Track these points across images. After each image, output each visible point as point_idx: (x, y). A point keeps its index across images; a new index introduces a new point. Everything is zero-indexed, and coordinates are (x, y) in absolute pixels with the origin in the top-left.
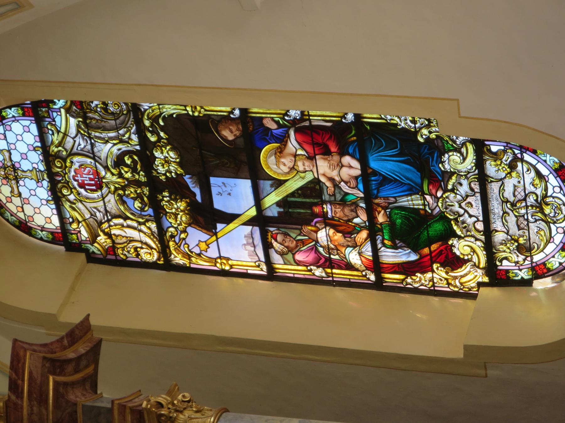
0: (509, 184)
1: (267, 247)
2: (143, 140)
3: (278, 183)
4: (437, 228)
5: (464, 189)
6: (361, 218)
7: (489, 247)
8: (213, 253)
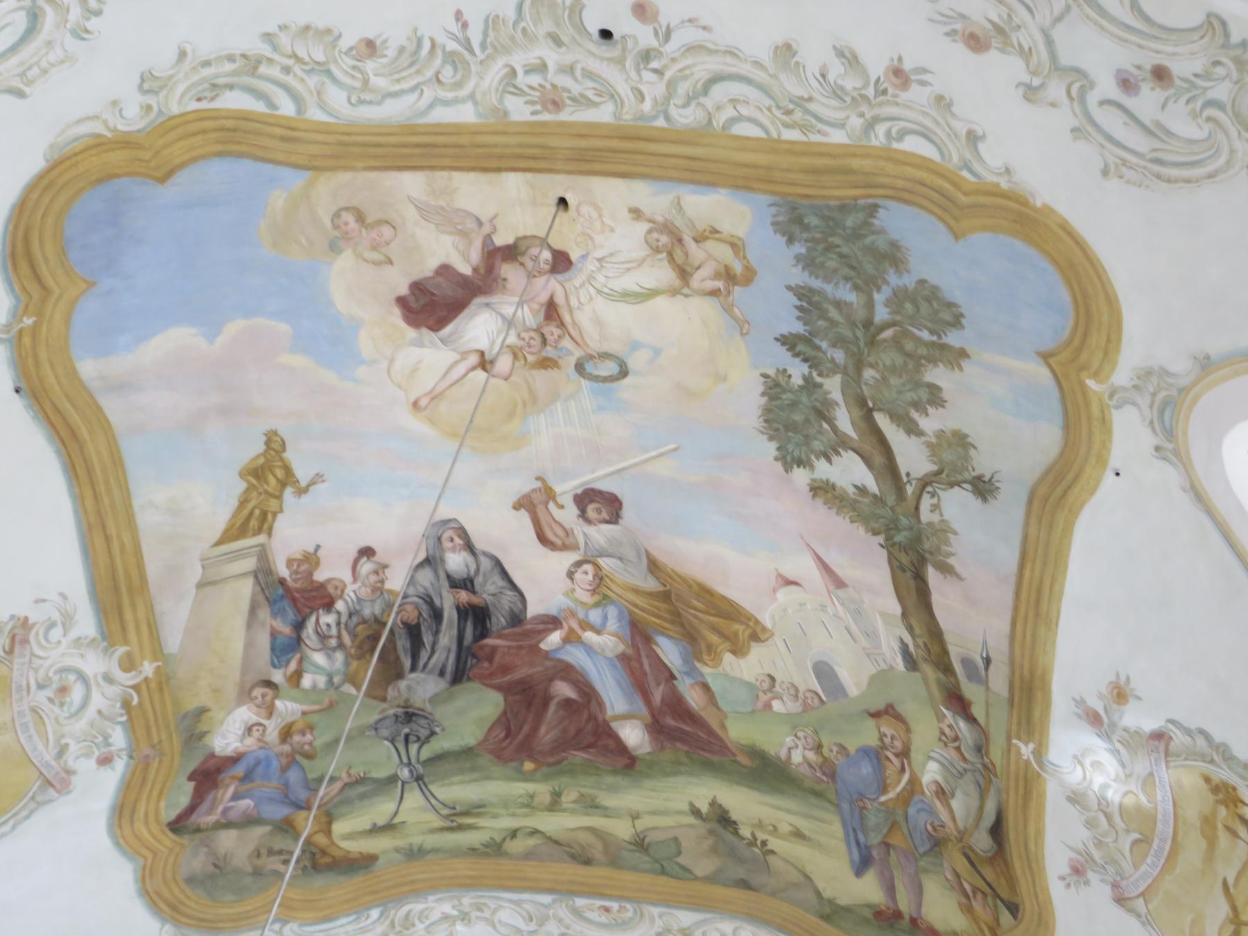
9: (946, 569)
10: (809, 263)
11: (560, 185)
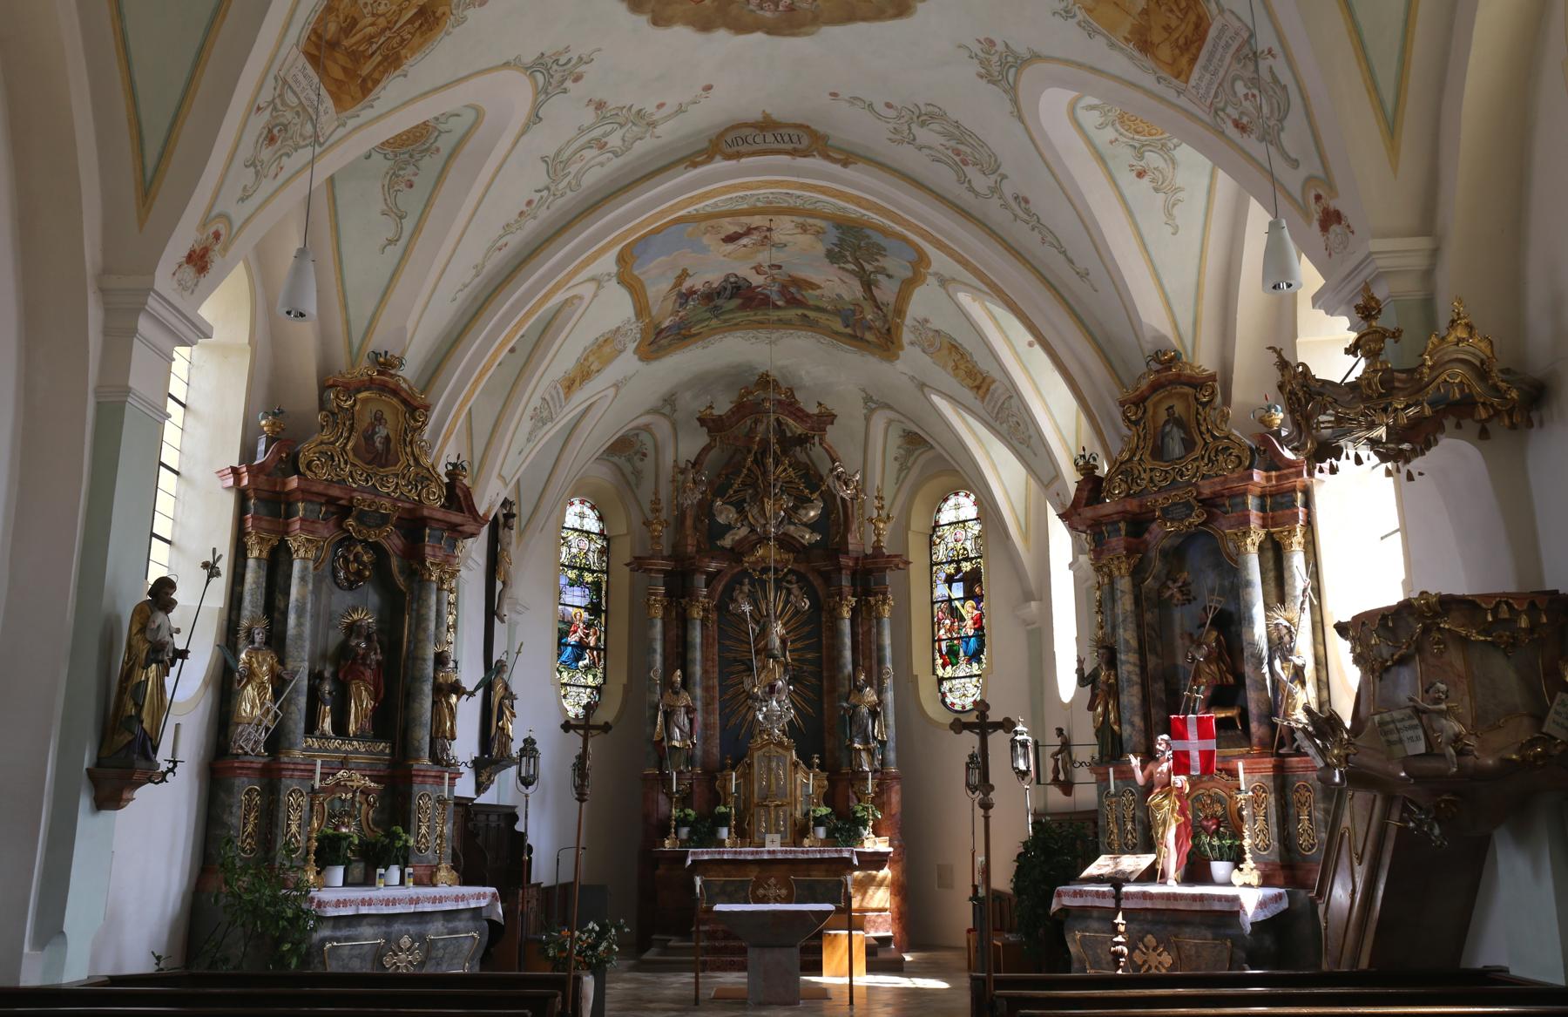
0: (970, 685)
1: (942, 602)
2: (973, 559)
3: (963, 607)
5: (967, 670)
6: (955, 636)
8: (938, 582)
9: (877, 287)
10: (843, 233)
11: (770, 217)
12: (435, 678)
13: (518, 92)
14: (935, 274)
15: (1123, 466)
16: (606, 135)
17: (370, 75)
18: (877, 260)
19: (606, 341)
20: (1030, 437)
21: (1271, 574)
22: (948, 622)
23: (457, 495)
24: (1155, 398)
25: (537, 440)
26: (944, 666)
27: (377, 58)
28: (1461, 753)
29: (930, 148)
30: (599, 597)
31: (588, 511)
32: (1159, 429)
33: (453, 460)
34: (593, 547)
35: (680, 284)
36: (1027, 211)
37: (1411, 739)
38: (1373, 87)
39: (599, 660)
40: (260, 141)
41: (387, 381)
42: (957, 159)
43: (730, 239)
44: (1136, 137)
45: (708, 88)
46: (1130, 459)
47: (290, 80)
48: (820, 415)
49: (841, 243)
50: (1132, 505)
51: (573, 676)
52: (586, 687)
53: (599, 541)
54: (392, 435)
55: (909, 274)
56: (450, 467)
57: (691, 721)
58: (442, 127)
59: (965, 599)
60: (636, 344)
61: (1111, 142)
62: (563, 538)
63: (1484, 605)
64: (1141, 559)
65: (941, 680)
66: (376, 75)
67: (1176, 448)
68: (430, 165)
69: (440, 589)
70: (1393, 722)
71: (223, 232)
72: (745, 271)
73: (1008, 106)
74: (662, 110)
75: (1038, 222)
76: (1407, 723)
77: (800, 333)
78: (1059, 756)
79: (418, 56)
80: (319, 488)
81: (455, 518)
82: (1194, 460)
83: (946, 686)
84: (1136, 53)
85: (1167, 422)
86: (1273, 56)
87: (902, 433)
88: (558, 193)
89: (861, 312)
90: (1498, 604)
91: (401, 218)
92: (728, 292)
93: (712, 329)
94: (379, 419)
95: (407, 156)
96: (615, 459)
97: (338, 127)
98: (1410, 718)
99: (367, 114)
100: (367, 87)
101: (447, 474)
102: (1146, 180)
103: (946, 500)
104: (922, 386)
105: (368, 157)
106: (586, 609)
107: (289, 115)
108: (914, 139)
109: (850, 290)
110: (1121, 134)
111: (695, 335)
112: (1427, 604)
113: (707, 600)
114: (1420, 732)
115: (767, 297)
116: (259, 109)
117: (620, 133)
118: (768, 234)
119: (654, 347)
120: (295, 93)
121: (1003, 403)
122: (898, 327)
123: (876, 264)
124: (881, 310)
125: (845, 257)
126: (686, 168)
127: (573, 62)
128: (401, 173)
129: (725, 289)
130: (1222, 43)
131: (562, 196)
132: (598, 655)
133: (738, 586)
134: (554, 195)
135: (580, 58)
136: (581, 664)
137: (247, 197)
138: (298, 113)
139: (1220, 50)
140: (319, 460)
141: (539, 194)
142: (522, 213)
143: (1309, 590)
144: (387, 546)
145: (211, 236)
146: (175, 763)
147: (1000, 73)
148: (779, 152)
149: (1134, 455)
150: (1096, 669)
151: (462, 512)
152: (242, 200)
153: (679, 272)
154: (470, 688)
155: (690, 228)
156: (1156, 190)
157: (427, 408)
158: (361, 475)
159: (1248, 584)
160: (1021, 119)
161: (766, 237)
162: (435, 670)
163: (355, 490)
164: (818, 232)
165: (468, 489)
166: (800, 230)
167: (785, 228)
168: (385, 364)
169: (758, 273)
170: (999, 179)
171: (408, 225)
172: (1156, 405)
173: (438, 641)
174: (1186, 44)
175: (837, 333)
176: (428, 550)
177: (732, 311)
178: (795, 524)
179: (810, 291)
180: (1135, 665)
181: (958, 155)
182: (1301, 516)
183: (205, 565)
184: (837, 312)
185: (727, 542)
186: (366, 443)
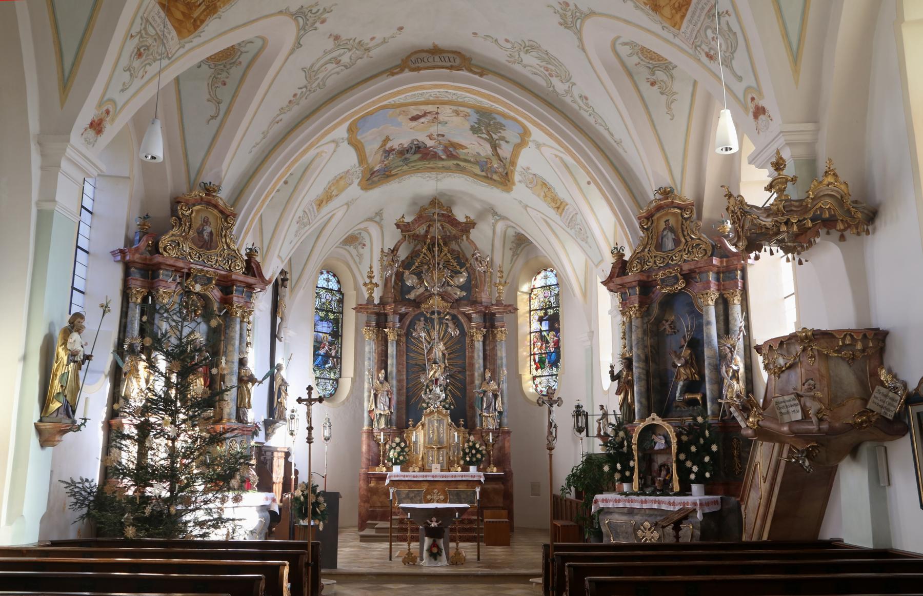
1: (536, 332)
2: (554, 307)
3: (548, 335)
4: (543, 366)
6: (543, 352)
7: (540, 376)
9: (500, 148)
11: (438, 106)
12: (239, 373)
13: (288, 31)
14: (534, 141)
15: (639, 254)
16: (340, 55)
17: (198, 17)
18: (500, 132)
19: (341, 178)
20: (587, 237)
21: (722, 318)
22: (539, 344)
23: (253, 268)
24: (658, 215)
25: (300, 236)
26: (537, 369)
27: (203, 7)
28: (821, 420)
29: (531, 66)
30: (338, 328)
31: (331, 278)
32: (660, 233)
33: (250, 246)
34: (334, 298)
35: (385, 145)
36: (587, 105)
37: (794, 411)
38: (786, 35)
39: (338, 364)
40: (133, 55)
41: (211, 199)
42: (547, 73)
43: (414, 118)
44: (651, 62)
45: (401, 29)
46: (643, 250)
47: (150, 19)
48: (466, 223)
49: (479, 122)
50: (644, 278)
51: (322, 373)
52: (330, 379)
53: (338, 295)
54: (214, 231)
55: (518, 141)
56: (248, 251)
57: (390, 399)
58: (243, 49)
59: (549, 331)
60: (359, 180)
61: (636, 65)
62: (317, 293)
63: (837, 336)
64: (648, 308)
65: (534, 378)
66: (202, 17)
67: (669, 244)
68: (236, 72)
69: (242, 322)
70: (784, 402)
71: (111, 110)
72: (422, 138)
73: (577, 42)
74: (373, 41)
75: (593, 111)
76: (792, 403)
77: (455, 175)
78: (601, 421)
79: (227, 6)
80: (171, 262)
81: (251, 280)
82: (680, 251)
83: (538, 380)
84: (650, 12)
85: (665, 229)
86: (729, 15)
87: (514, 234)
88: (312, 90)
89: (491, 163)
90: (845, 335)
91: (219, 103)
92: (413, 150)
93: (404, 172)
94: (206, 222)
95: (222, 66)
96: (347, 247)
97: (179, 48)
98: (794, 399)
99: (197, 41)
100: (197, 24)
101: (247, 254)
102: (656, 87)
103: (539, 273)
104: (526, 207)
105: (199, 66)
106: (330, 334)
107: (150, 41)
108: (522, 61)
109: (486, 150)
110: (642, 60)
111: (394, 175)
112: (806, 335)
113: (399, 330)
114: (799, 408)
115: (436, 153)
116: (132, 36)
117: (349, 54)
118: (436, 116)
119: (370, 182)
120: (153, 27)
121: (572, 217)
122: (512, 171)
123: (499, 134)
124: (502, 161)
125: (481, 130)
126: (387, 76)
127: (320, 12)
128: (219, 76)
129: (411, 148)
130: (700, 6)
131: (314, 91)
132: (337, 361)
133: (417, 322)
134: (310, 91)
135: (325, 9)
136: (327, 366)
137: (126, 89)
138: (155, 39)
139: (699, 11)
140: (171, 245)
141: (301, 90)
142: (290, 101)
143: (743, 328)
144: (211, 297)
145: (104, 112)
146: (85, 420)
147: (572, 22)
148: (442, 67)
149: (645, 248)
150: (621, 371)
151: (255, 276)
152: (123, 91)
153: (384, 138)
154: (260, 379)
155: (391, 112)
156: (662, 93)
157: (235, 216)
158: (196, 255)
159: (709, 323)
160: (584, 50)
161: (435, 118)
162: (239, 369)
163: (192, 263)
164: (466, 115)
165: (258, 263)
166: (455, 114)
167: (446, 112)
168: (210, 190)
169: (431, 139)
170: (571, 85)
171: (223, 107)
172: (658, 219)
173: (241, 352)
174: (679, 7)
175: (476, 175)
176: (235, 299)
177: (415, 161)
178: (451, 286)
179: (461, 150)
180: (643, 369)
181: (547, 71)
182: (740, 284)
183: (102, 306)
184: (477, 163)
185: (412, 296)
186: (199, 236)
